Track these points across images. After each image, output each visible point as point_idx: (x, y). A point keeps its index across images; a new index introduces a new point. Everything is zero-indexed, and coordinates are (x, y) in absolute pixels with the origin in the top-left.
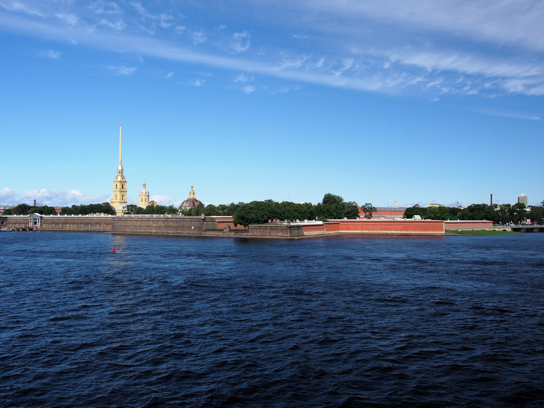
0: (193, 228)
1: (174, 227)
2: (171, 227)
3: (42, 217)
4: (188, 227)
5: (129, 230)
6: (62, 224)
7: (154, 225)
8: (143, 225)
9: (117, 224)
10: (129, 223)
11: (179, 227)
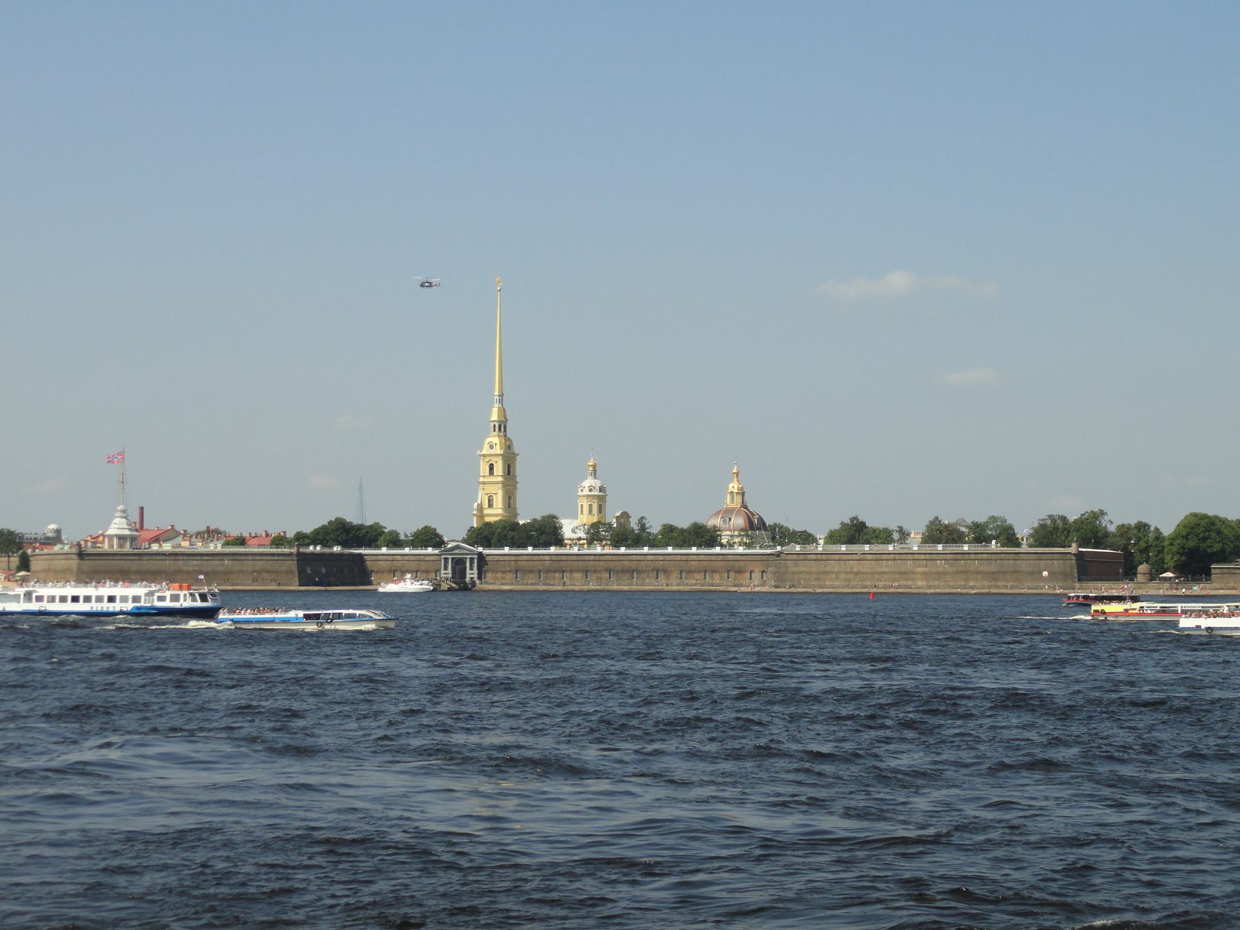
0: (1045, 574)
1: (987, 573)
2: (977, 573)
3: (480, 554)
4: (1032, 573)
5: (837, 583)
6: (548, 571)
7: (920, 569)
8: (884, 569)
9: (791, 570)
10: (834, 566)
11: (1004, 573)
